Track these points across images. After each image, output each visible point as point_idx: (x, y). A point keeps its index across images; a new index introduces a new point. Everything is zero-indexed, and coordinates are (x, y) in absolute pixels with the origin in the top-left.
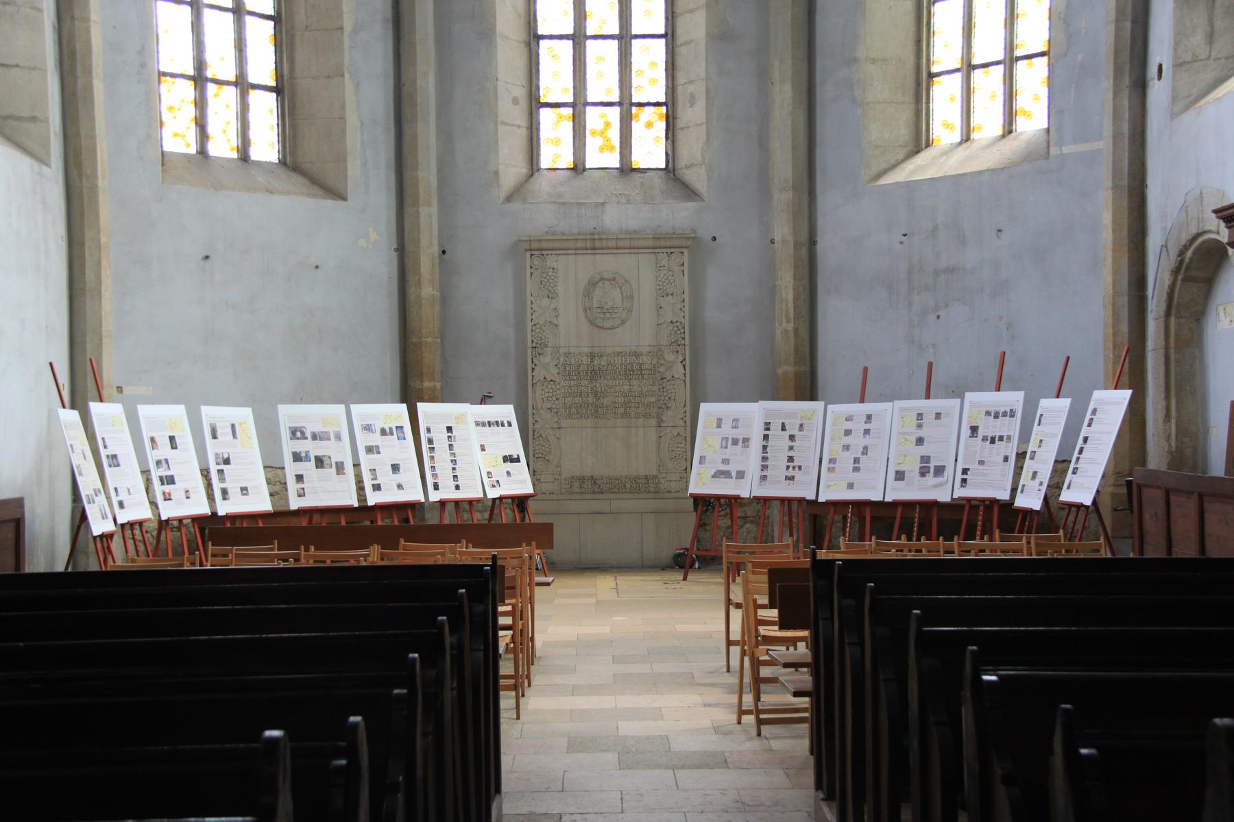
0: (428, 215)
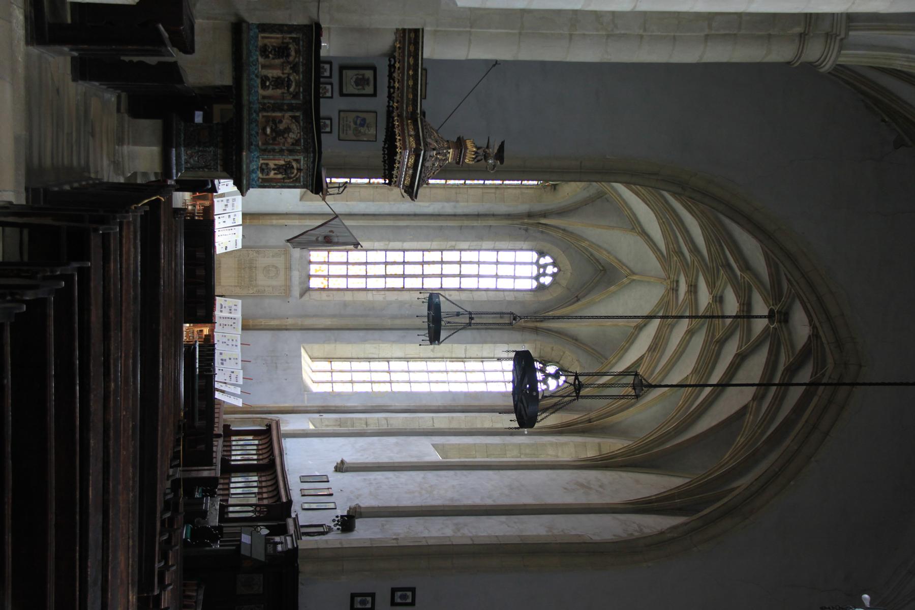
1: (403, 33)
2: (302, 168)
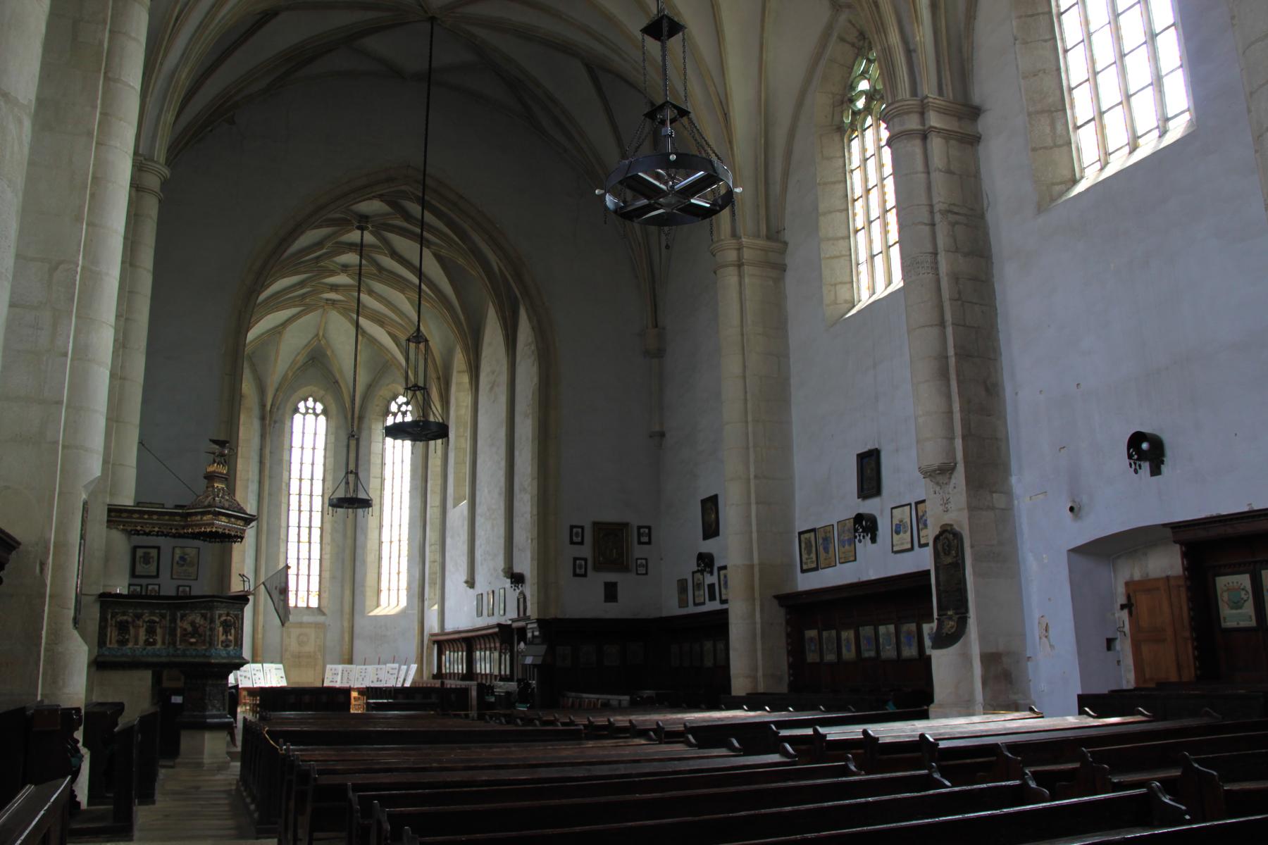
0: (261, 618)
1: (111, 523)
2: (226, 612)
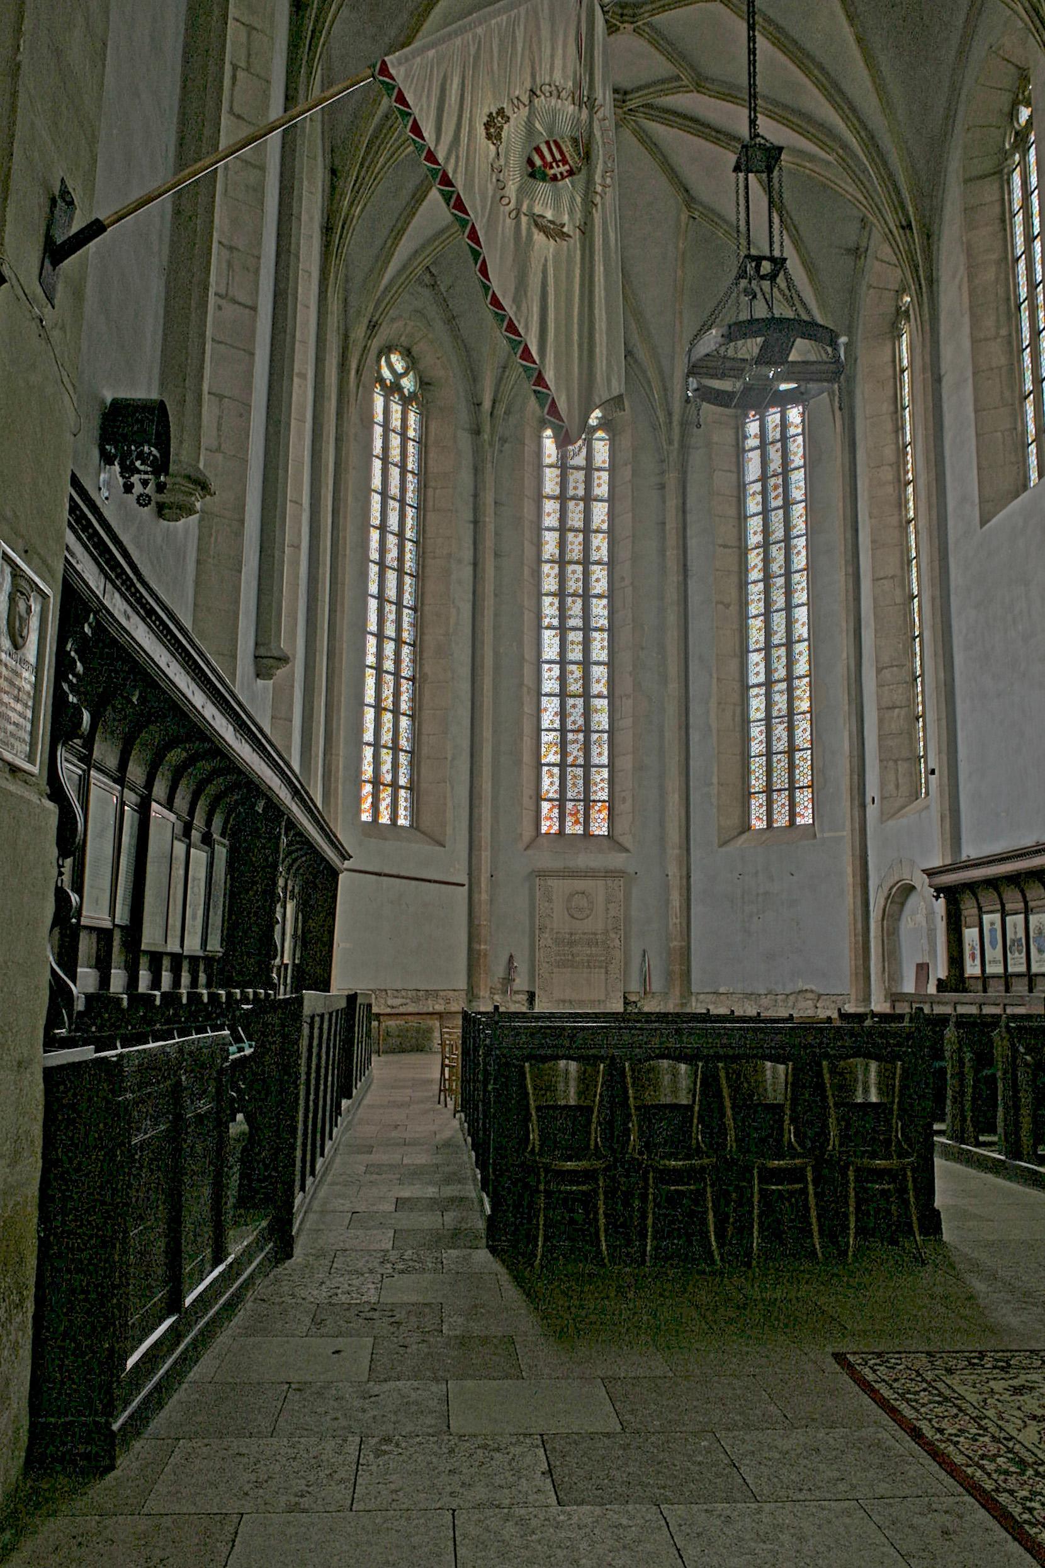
0: (486, 855)
